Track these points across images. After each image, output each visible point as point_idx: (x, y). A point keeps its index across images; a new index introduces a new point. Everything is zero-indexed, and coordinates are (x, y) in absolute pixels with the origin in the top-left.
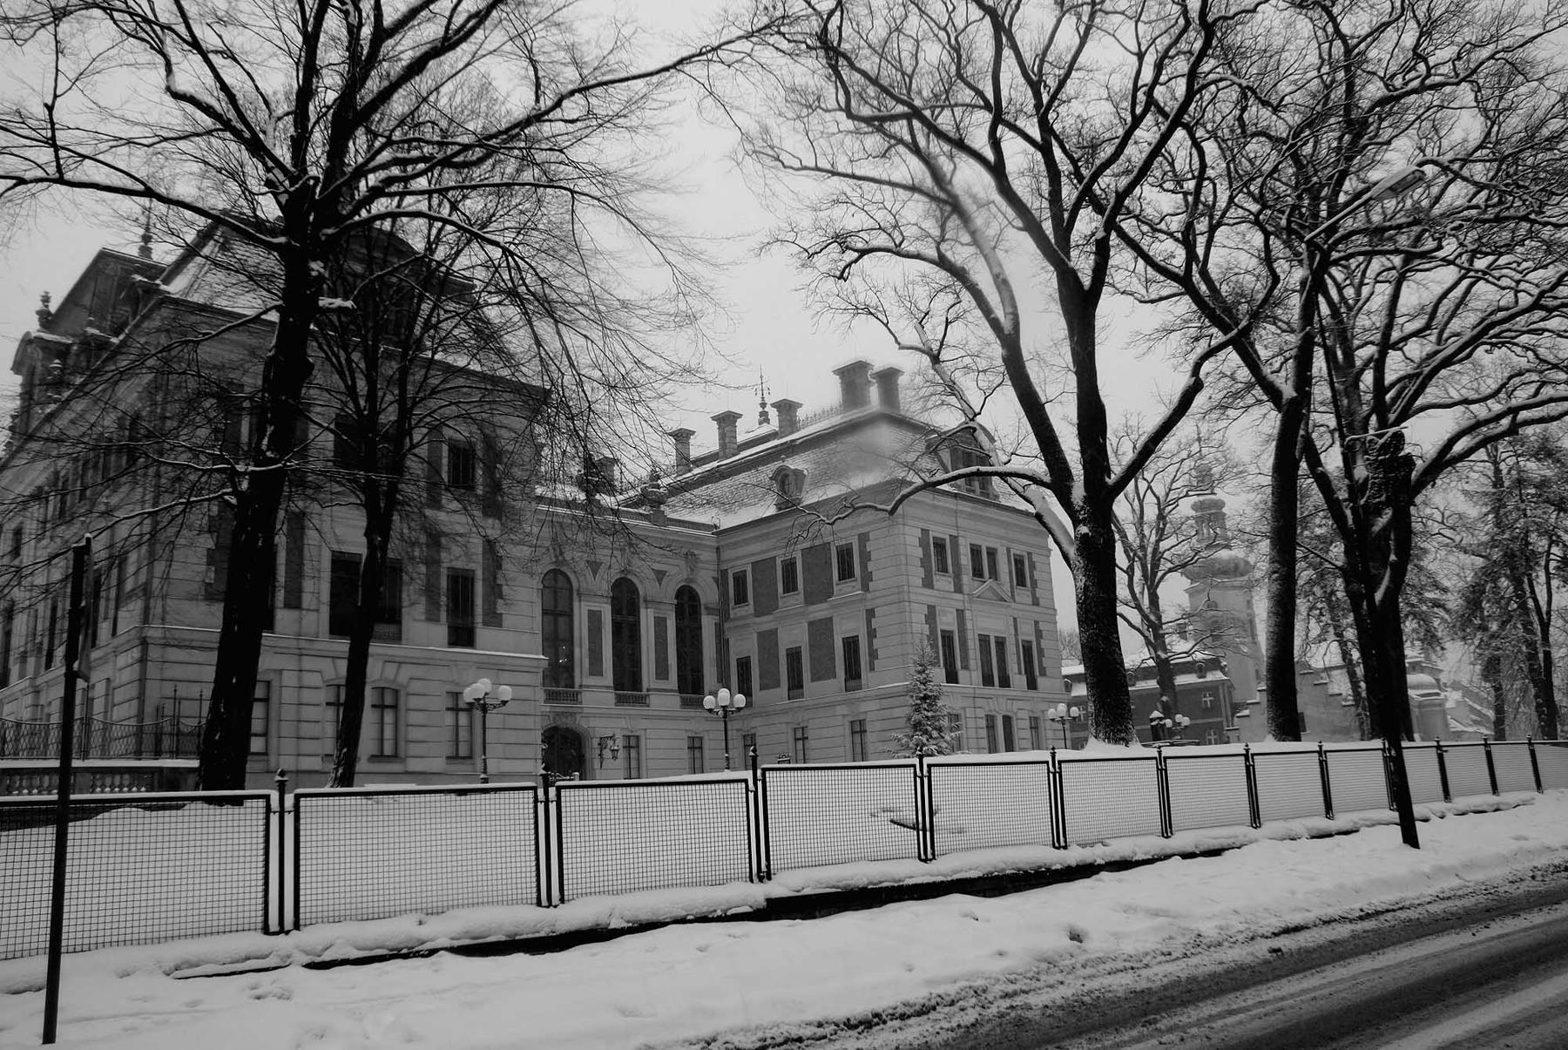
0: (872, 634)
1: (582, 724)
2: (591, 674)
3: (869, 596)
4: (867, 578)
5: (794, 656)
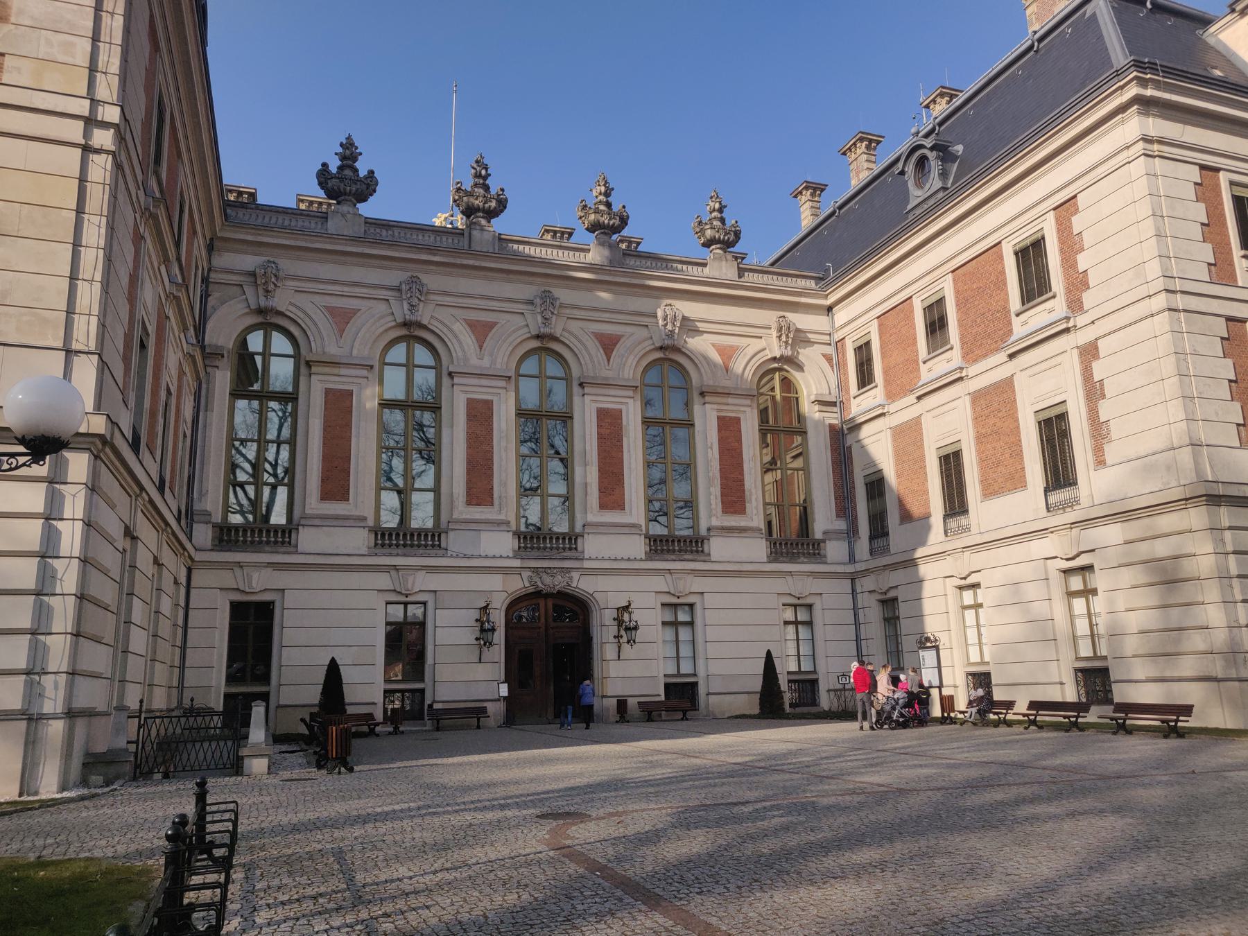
0: (1094, 392)
1: (584, 585)
2: (603, 506)
3: (1081, 320)
4: (1078, 284)
5: (951, 463)
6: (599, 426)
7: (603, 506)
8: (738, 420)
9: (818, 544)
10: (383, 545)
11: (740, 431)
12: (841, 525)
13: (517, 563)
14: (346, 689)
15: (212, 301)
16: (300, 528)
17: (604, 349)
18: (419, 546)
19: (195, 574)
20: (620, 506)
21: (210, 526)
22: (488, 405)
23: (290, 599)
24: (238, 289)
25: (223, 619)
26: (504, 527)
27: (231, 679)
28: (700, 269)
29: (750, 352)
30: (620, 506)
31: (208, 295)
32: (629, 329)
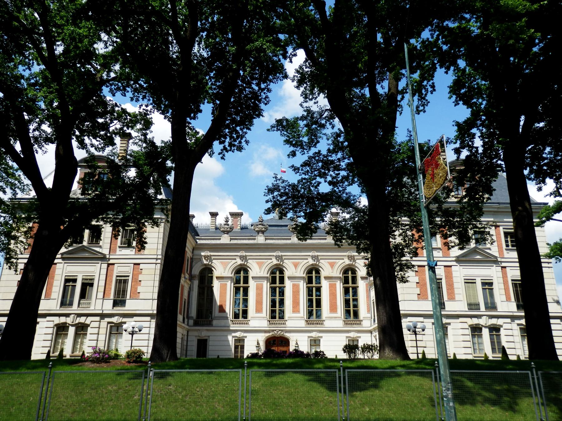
1: (287, 335)
2: (294, 312)
7: (294, 312)
12: (369, 315)
13: (268, 329)
15: (194, 263)
20: (298, 312)
23: (211, 338)
25: (195, 343)
30: (298, 312)
32: (302, 261)
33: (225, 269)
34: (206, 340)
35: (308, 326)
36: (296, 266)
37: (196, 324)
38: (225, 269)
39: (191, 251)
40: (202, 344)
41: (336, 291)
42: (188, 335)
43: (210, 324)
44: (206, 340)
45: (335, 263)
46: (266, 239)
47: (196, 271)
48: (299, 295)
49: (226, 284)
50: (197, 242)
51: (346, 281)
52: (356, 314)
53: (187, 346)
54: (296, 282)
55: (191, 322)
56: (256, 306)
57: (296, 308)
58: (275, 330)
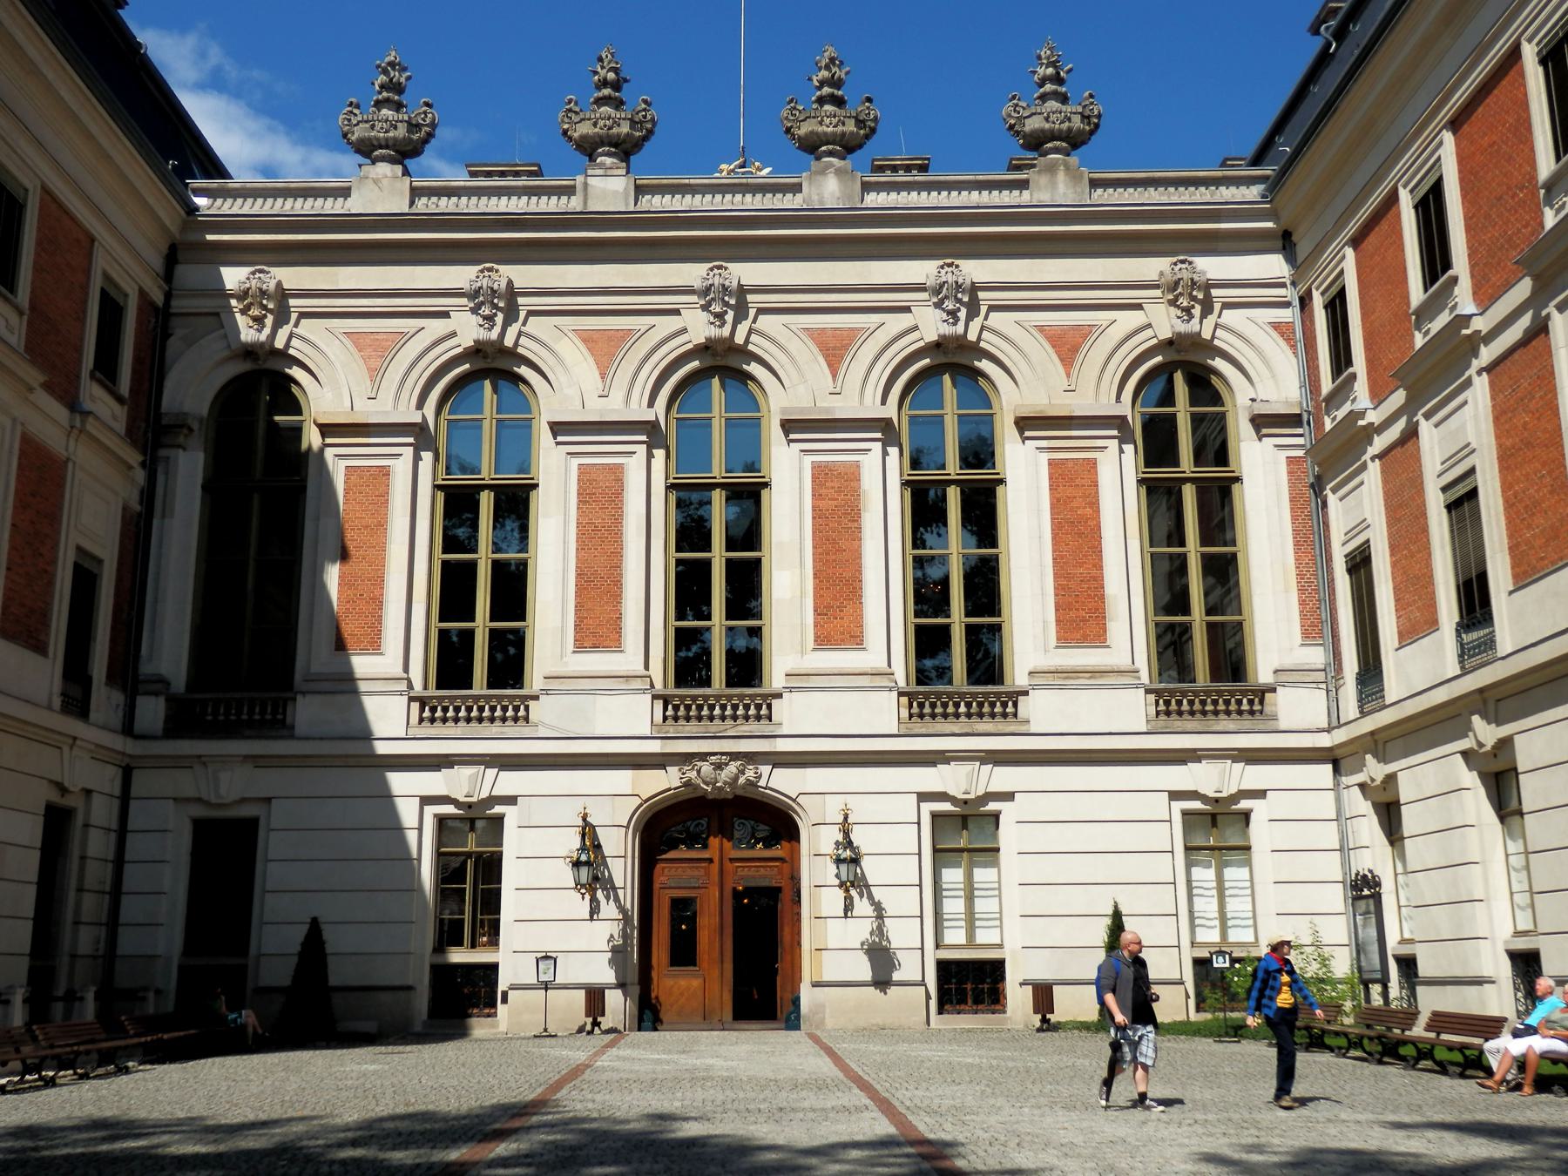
1: (782, 782)
2: (824, 640)
6: (816, 496)
7: (824, 640)
8: (1093, 464)
9: (1262, 693)
10: (432, 720)
11: (1095, 484)
12: (1316, 656)
13: (654, 747)
14: (332, 963)
15: (173, 344)
16: (299, 698)
17: (826, 357)
18: (492, 720)
19: (136, 775)
20: (853, 638)
21: (161, 701)
22: (617, 473)
23: (279, 815)
24: (211, 319)
25: (178, 846)
26: (637, 684)
27: (190, 947)
28: (1016, 193)
29: (1116, 333)
30: (853, 638)
31: (166, 335)
33: (376, 375)
34: (251, 825)
35: (918, 727)
36: (835, 351)
37: (186, 719)
38: (376, 375)
39: (158, 263)
40: (226, 854)
41: (1094, 504)
42: (125, 798)
43: (276, 724)
44: (251, 825)
45: (1084, 332)
46: (640, 190)
47: (192, 388)
48: (856, 534)
49: (385, 472)
50: (192, 210)
51: (1157, 442)
52: (1230, 660)
53: (119, 862)
54: (834, 451)
55: (152, 711)
56: (579, 607)
57: (837, 618)
58: (703, 756)
